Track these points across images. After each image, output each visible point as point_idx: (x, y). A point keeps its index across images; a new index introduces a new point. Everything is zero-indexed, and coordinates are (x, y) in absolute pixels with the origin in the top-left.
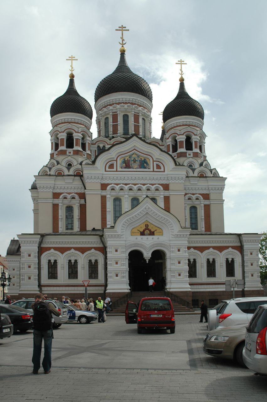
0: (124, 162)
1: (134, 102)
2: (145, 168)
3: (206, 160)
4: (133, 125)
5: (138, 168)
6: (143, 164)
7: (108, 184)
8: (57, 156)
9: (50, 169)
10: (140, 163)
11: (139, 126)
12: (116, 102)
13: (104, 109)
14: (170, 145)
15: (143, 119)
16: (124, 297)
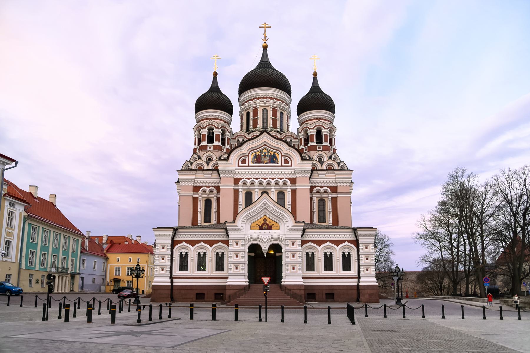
0: (256, 157)
1: (272, 97)
2: (274, 162)
3: (335, 152)
4: (272, 119)
6: (273, 159)
7: (241, 179)
8: (199, 151)
9: (191, 163)
11: (277, 119)
12: (256, 97)
13: (246, 104)
14: (302, 138)
16: (242, 290)
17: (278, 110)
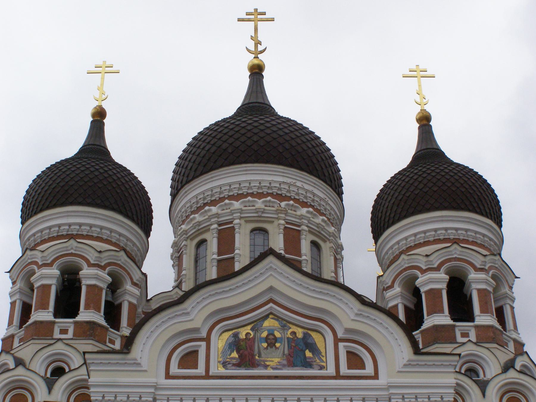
1: (284, 192)
2: (308, 364)
5: (281, 366)
10: (290, 347)
12: (231, 194)
13: (194, 218)
14: (396, 306)
15: (314, 243)
17: (305, 233)
